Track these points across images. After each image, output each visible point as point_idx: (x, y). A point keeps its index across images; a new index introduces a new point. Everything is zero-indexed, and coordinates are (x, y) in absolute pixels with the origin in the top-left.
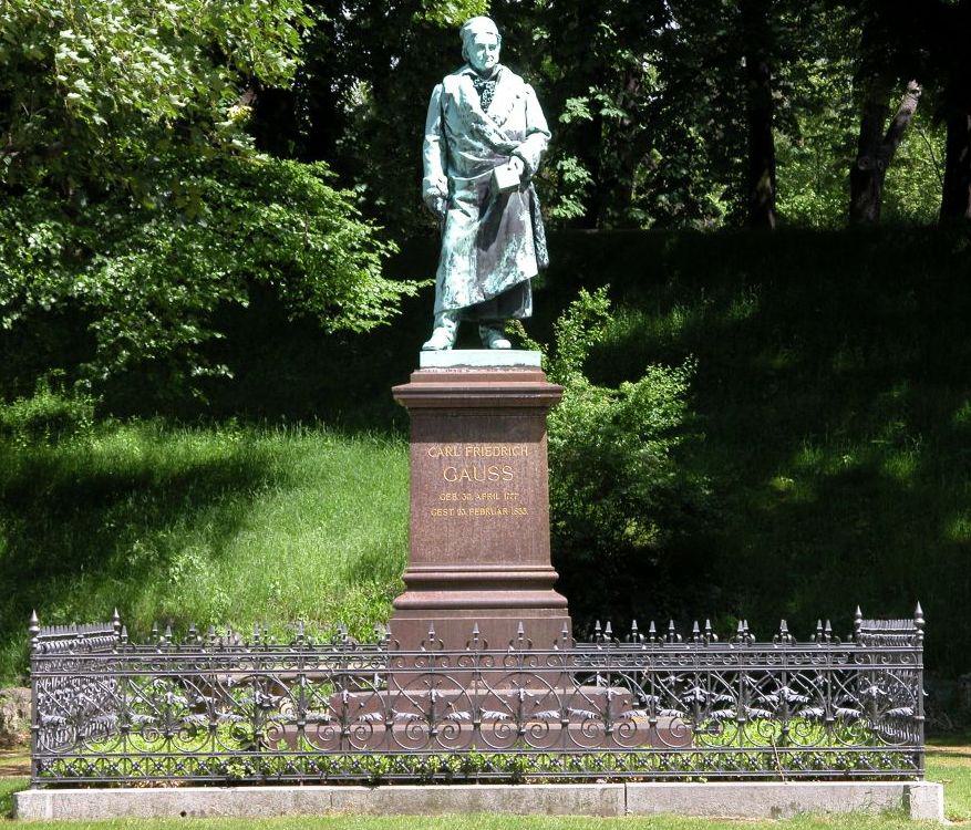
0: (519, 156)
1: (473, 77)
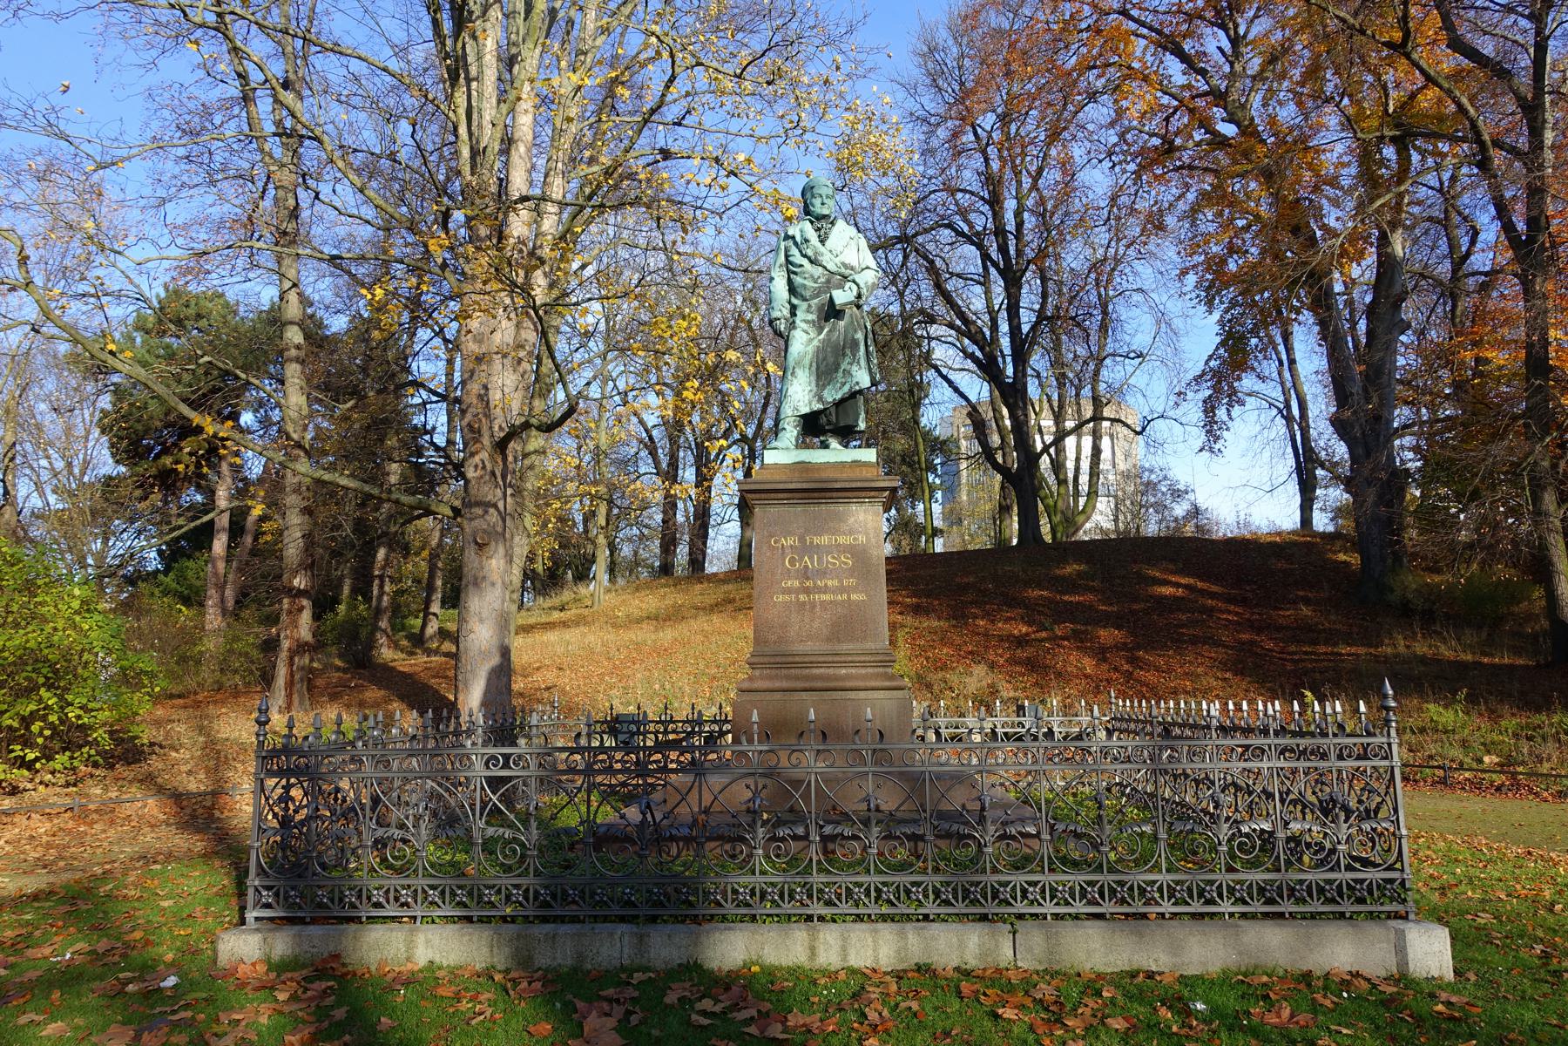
0: (854, 282)
1: (812, 222)
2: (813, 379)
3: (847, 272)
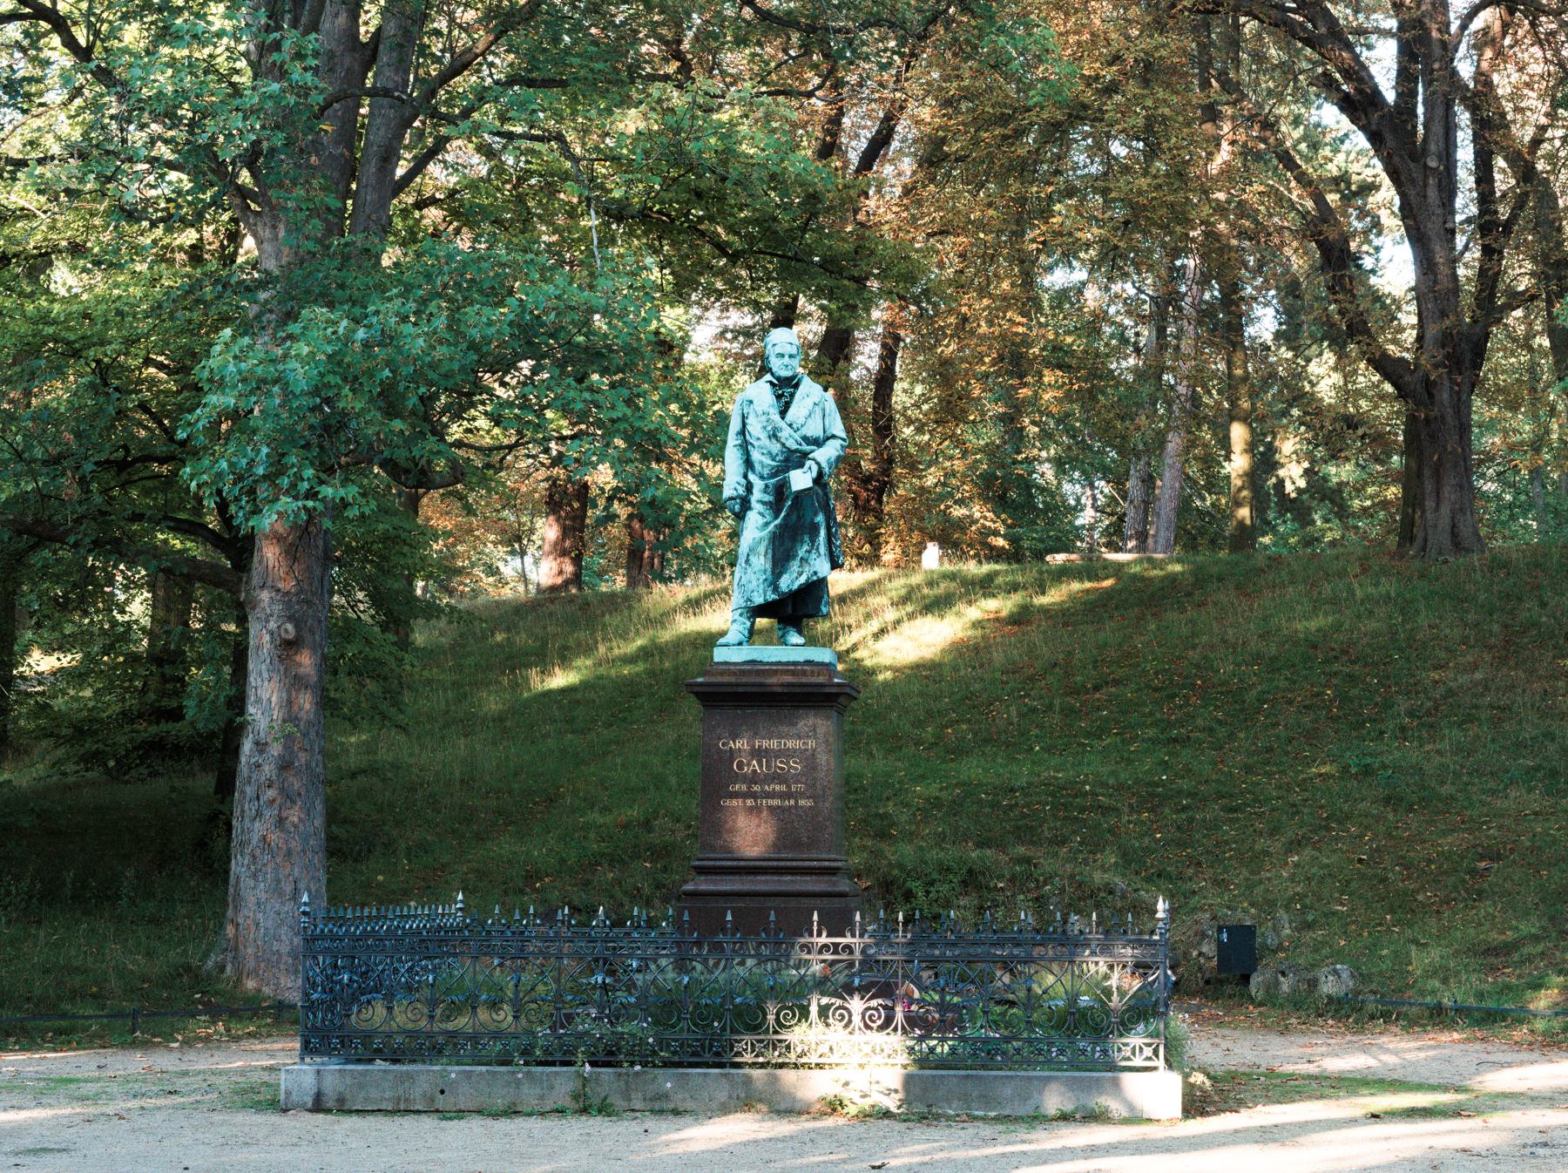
2: (769, 566)
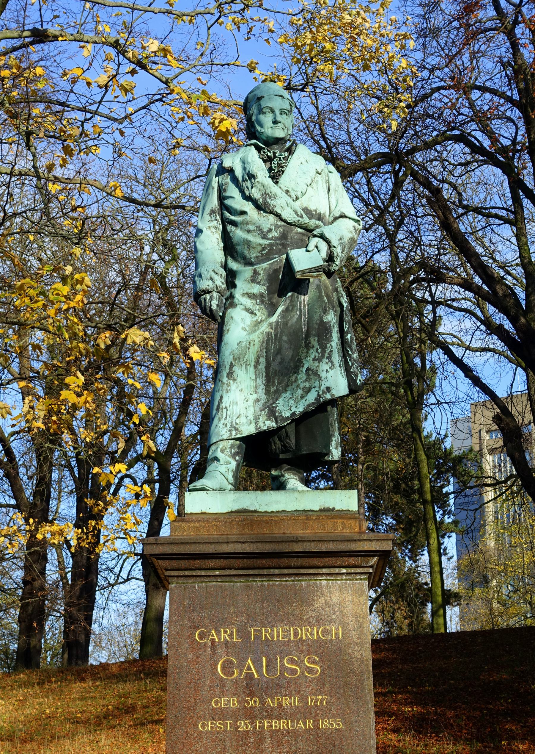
0: (322, 237)
1: (258, 149)
2: (261, 382)
3: (313, 223)
